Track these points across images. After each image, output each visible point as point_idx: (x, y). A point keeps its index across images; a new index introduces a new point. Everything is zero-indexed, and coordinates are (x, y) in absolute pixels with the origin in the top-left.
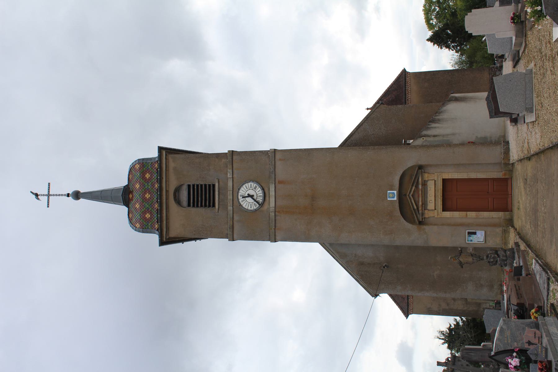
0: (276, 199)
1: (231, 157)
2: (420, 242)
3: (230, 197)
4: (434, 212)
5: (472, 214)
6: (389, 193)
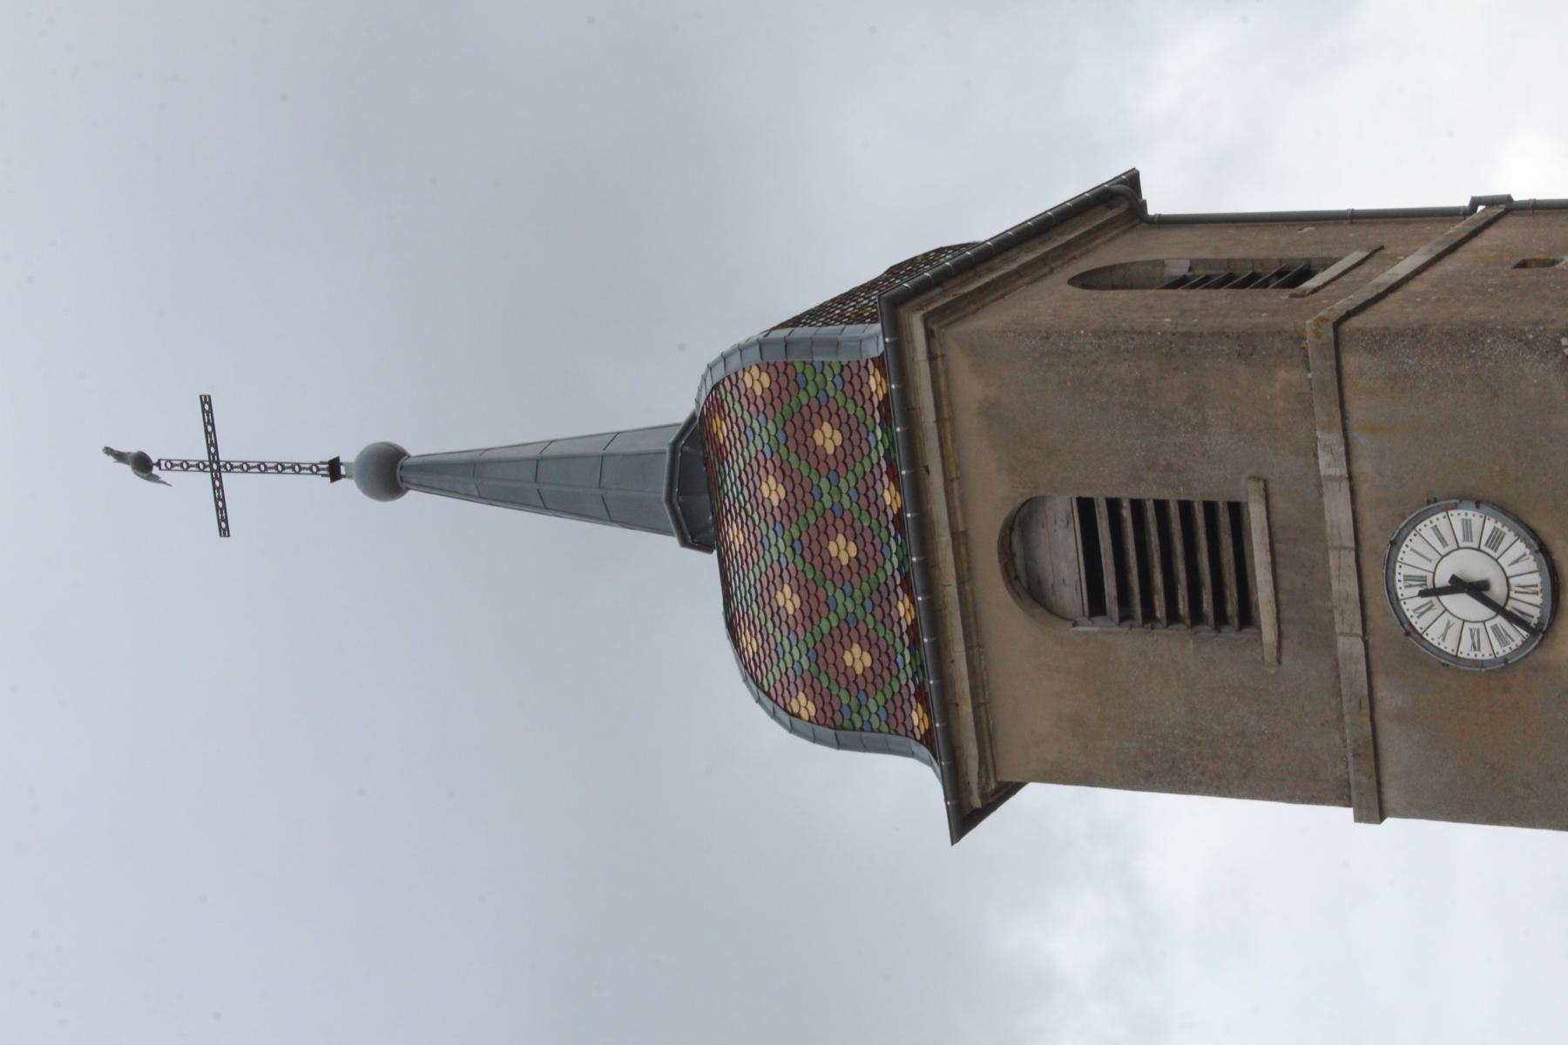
1: (1333, 362)
3: (1344, 585)
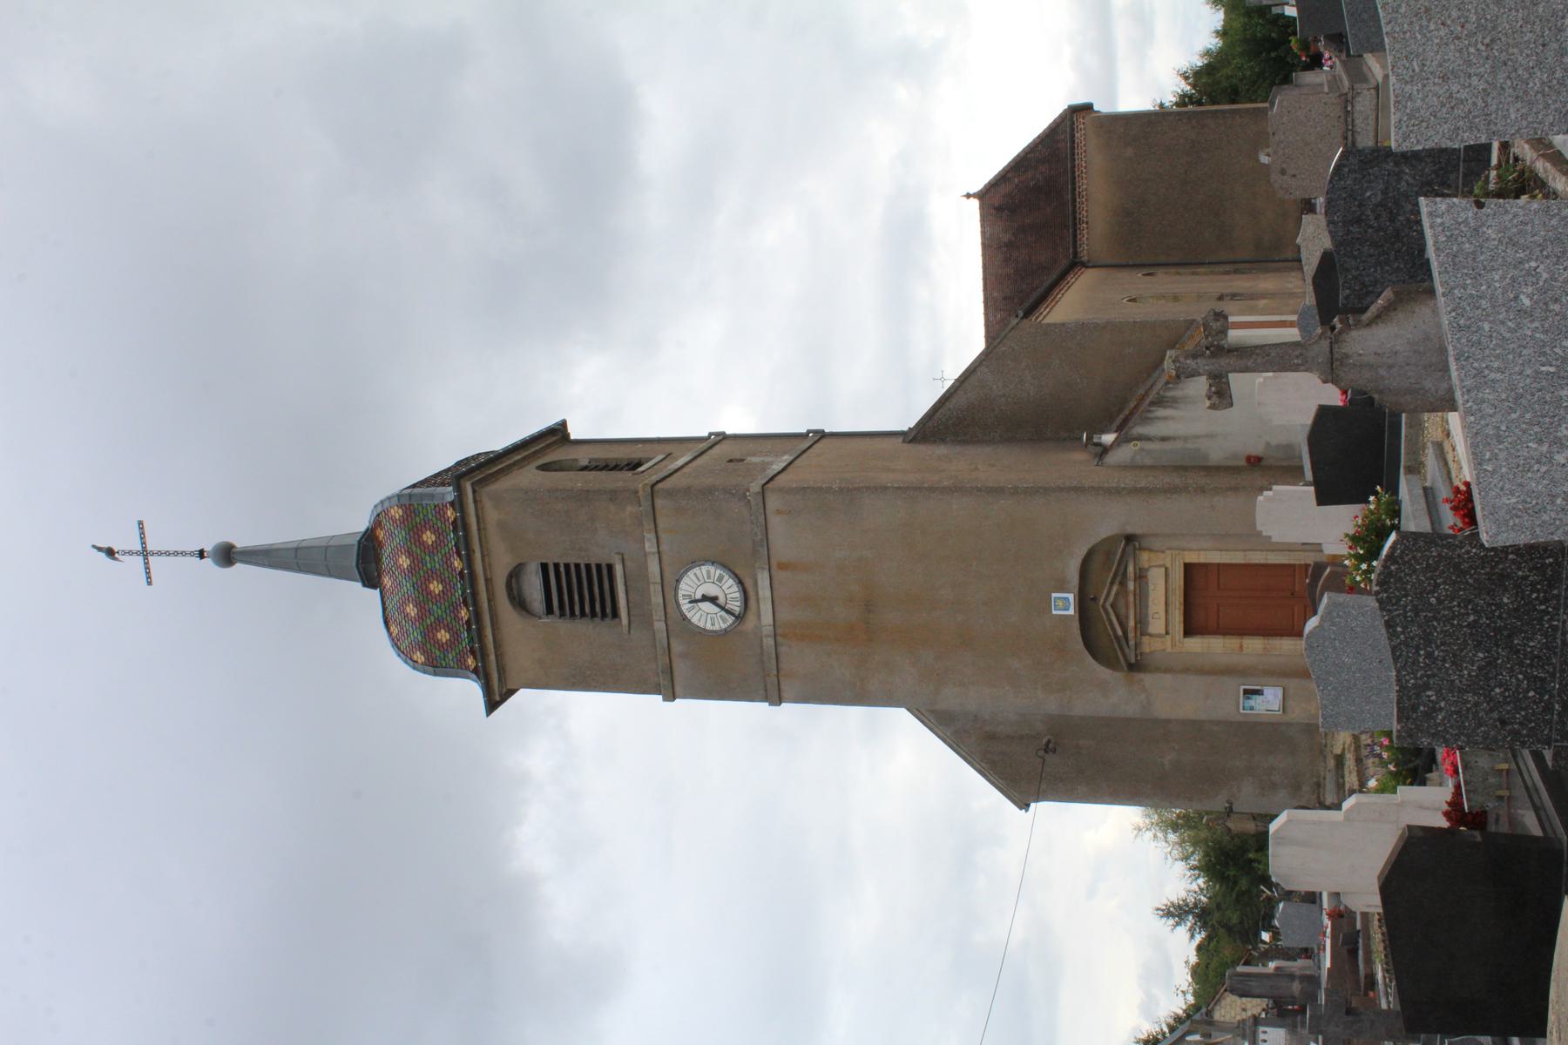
0: (776, 604)
1: (650, 503)
2: (1131, 710)
3: (657, 599)
4: (1163, 639)
5: (1254, 645)
6: (1055, 598)
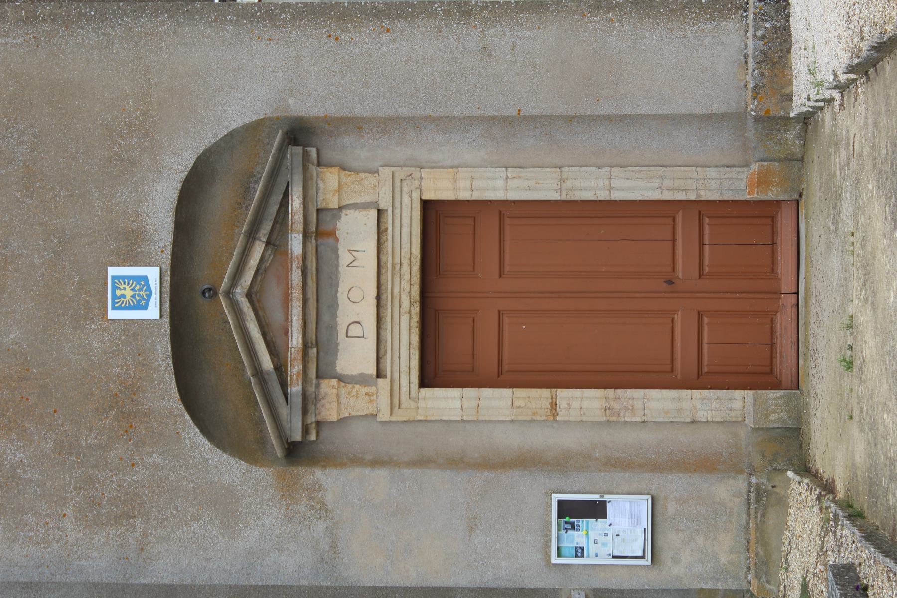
4: (373, 389)
6: (113, 277)
